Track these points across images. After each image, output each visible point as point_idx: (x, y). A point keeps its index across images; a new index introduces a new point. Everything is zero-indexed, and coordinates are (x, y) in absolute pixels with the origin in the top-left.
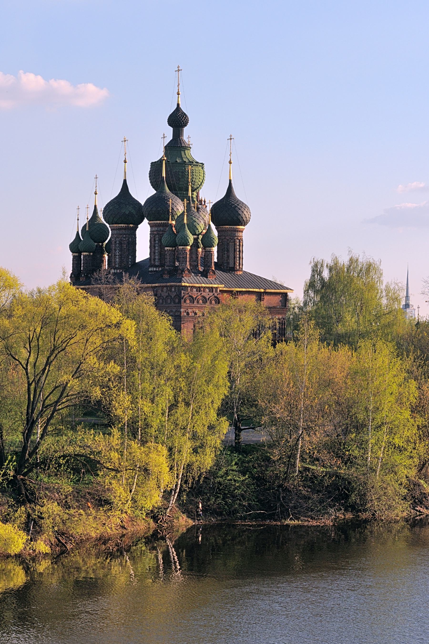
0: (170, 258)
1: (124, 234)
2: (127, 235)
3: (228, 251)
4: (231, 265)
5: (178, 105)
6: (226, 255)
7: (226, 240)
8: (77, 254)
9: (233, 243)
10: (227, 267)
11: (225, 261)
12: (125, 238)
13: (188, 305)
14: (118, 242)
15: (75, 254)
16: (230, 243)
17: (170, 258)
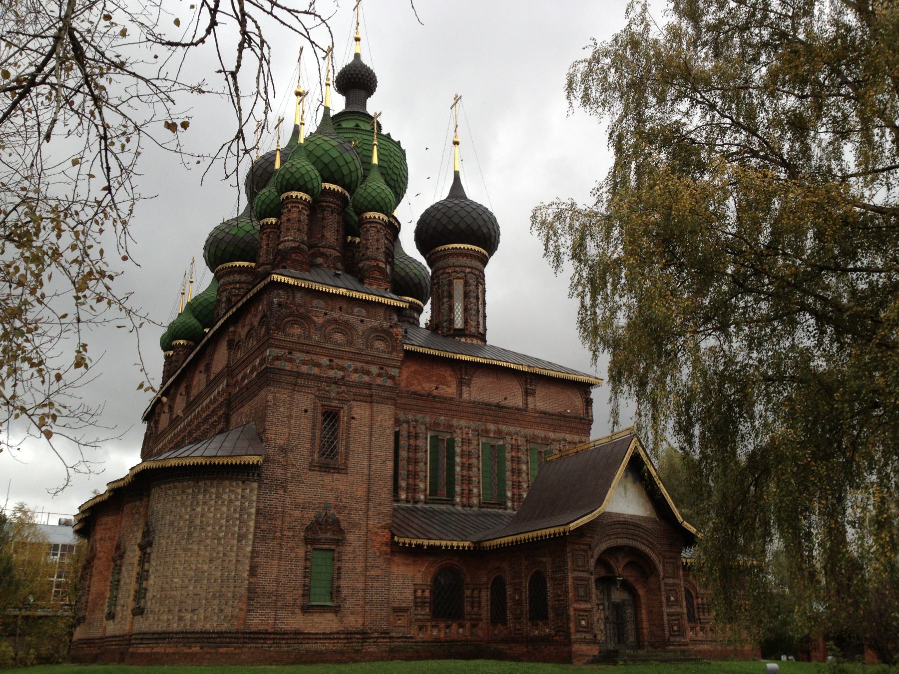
0: (268, 245)
1: (237, 283)
2: (244, 285)
3: (451, 296)
4: (459, 323)
5: (357, 56)
6: (446, 306)
7: (445, 276)
8: (171, 353)
9: (462, 281)
10: (449, 330)
11: (445, 318)
12: (239, 289)
13: (295, 339)
14: (224, 299)
15: (167, 353)
16: (455, 281)
17: (268, 245)
